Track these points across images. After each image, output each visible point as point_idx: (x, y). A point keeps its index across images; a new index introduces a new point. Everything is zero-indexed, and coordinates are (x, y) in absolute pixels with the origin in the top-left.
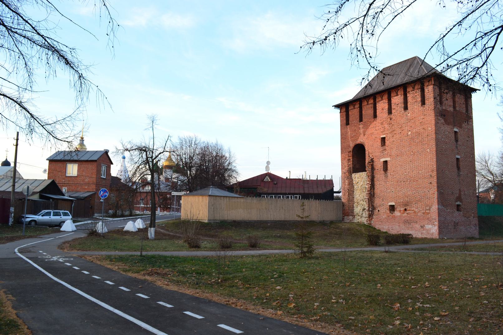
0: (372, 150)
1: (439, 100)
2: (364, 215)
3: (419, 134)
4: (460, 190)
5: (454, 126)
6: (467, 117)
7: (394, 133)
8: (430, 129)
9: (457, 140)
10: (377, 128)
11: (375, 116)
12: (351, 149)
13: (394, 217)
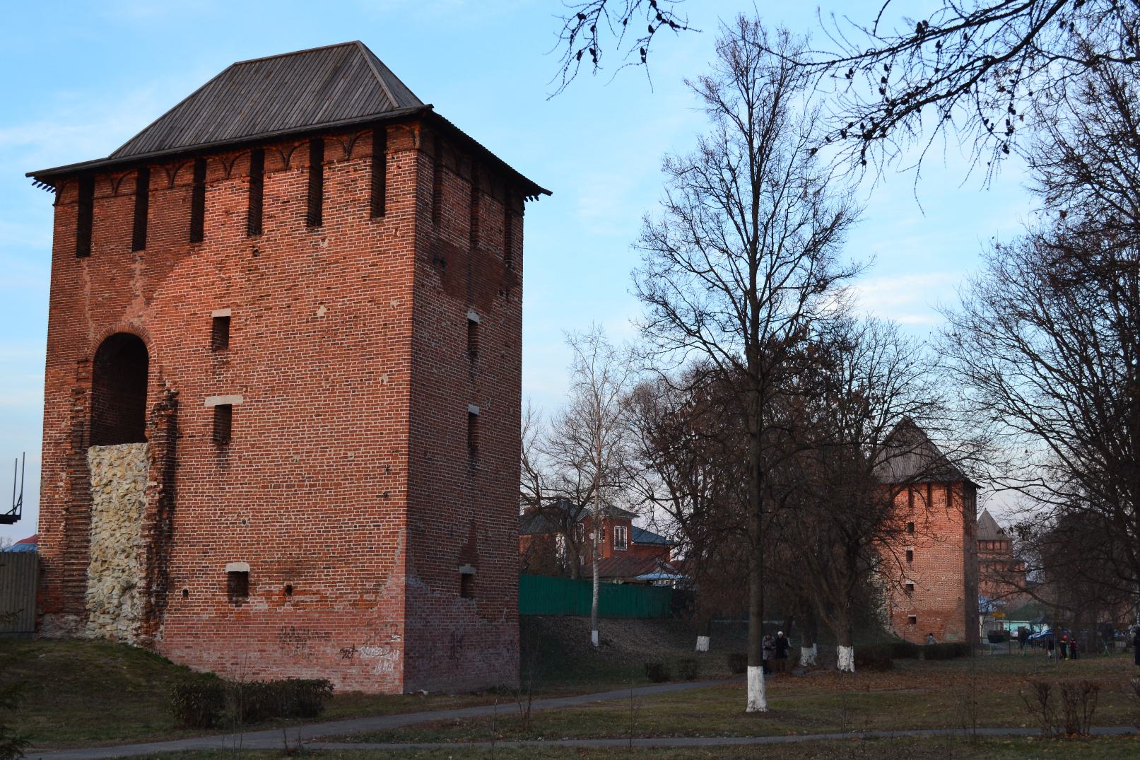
0: (174, 358)
1: (430, 208)
2: (127, 608)
3: (353, 317)
4: (472, 522)
5: (470, 302)
6: (508, 280)
7: (265, 304)
8: (394, 303)
9: (473, 354)
10: (201, 280)
11: (197, 234)
12: (89, 351)
13: (244, 618)
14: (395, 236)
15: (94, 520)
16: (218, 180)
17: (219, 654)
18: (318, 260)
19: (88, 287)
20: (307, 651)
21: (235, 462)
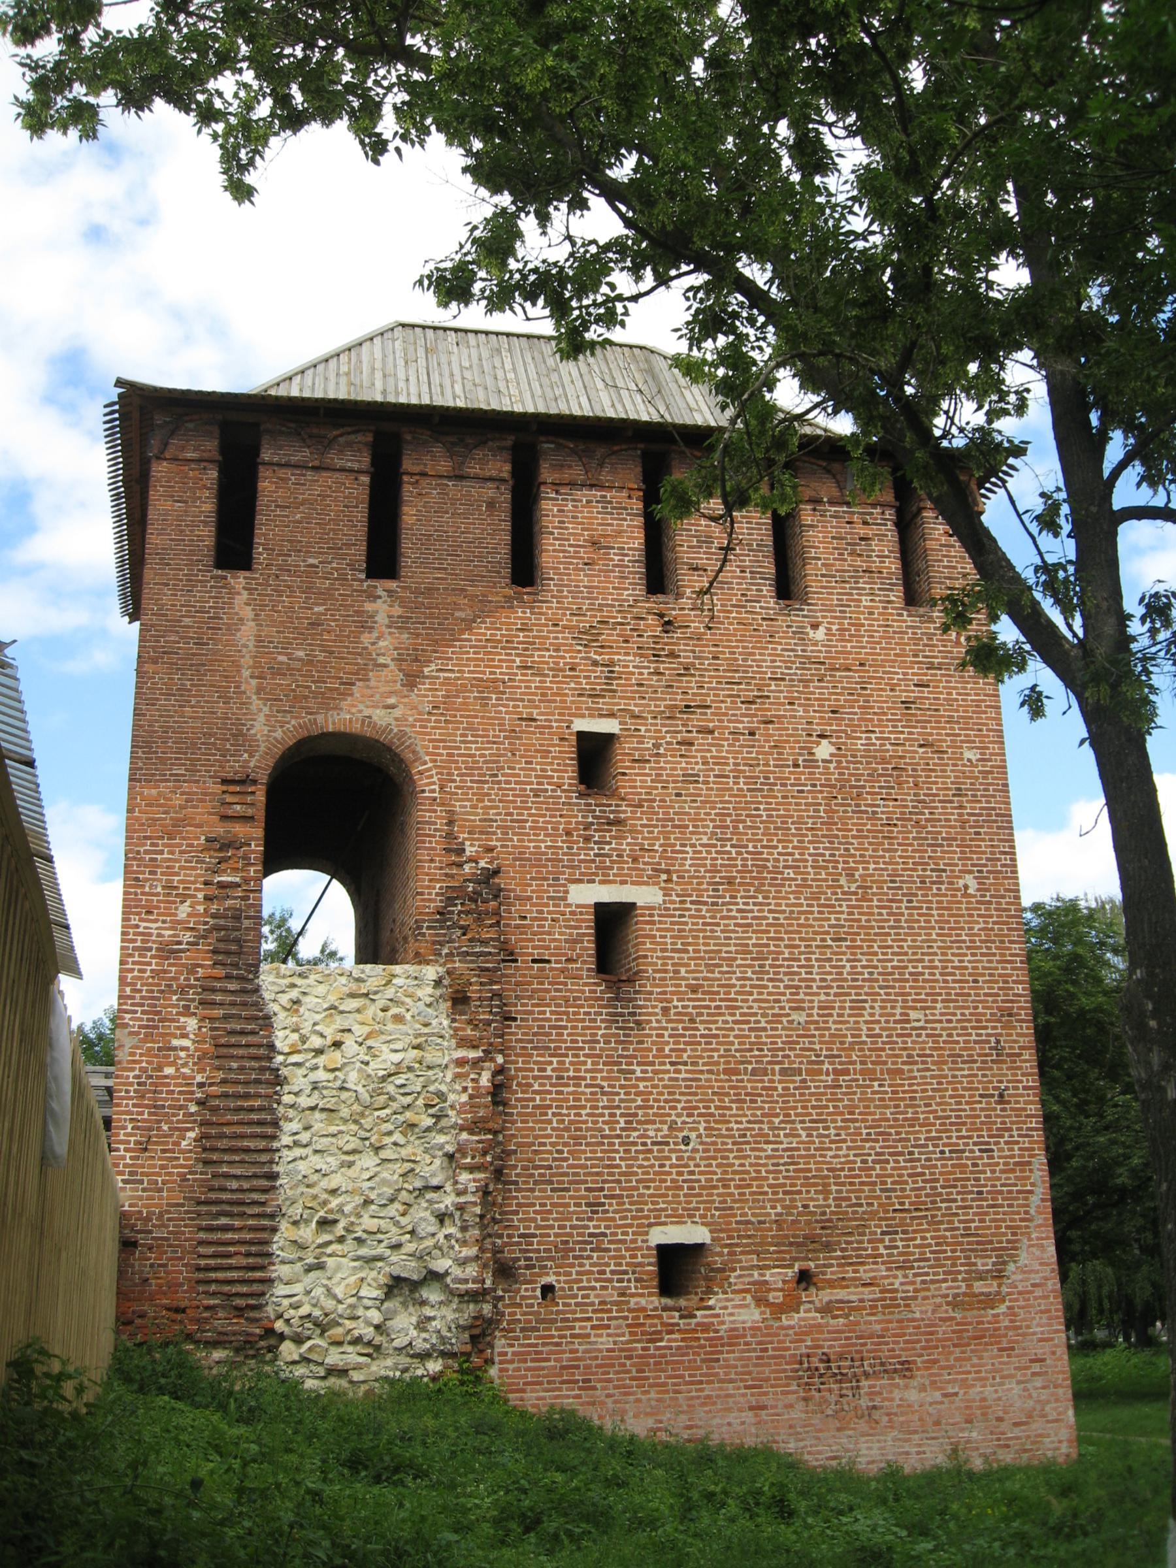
7: (696, 720)
11: (524, 569)
12: (259, 762)
15: (289, 1127)
16: (572, 484)
18: (809, 661)
19: (247, 634)
20: (864, 1402)
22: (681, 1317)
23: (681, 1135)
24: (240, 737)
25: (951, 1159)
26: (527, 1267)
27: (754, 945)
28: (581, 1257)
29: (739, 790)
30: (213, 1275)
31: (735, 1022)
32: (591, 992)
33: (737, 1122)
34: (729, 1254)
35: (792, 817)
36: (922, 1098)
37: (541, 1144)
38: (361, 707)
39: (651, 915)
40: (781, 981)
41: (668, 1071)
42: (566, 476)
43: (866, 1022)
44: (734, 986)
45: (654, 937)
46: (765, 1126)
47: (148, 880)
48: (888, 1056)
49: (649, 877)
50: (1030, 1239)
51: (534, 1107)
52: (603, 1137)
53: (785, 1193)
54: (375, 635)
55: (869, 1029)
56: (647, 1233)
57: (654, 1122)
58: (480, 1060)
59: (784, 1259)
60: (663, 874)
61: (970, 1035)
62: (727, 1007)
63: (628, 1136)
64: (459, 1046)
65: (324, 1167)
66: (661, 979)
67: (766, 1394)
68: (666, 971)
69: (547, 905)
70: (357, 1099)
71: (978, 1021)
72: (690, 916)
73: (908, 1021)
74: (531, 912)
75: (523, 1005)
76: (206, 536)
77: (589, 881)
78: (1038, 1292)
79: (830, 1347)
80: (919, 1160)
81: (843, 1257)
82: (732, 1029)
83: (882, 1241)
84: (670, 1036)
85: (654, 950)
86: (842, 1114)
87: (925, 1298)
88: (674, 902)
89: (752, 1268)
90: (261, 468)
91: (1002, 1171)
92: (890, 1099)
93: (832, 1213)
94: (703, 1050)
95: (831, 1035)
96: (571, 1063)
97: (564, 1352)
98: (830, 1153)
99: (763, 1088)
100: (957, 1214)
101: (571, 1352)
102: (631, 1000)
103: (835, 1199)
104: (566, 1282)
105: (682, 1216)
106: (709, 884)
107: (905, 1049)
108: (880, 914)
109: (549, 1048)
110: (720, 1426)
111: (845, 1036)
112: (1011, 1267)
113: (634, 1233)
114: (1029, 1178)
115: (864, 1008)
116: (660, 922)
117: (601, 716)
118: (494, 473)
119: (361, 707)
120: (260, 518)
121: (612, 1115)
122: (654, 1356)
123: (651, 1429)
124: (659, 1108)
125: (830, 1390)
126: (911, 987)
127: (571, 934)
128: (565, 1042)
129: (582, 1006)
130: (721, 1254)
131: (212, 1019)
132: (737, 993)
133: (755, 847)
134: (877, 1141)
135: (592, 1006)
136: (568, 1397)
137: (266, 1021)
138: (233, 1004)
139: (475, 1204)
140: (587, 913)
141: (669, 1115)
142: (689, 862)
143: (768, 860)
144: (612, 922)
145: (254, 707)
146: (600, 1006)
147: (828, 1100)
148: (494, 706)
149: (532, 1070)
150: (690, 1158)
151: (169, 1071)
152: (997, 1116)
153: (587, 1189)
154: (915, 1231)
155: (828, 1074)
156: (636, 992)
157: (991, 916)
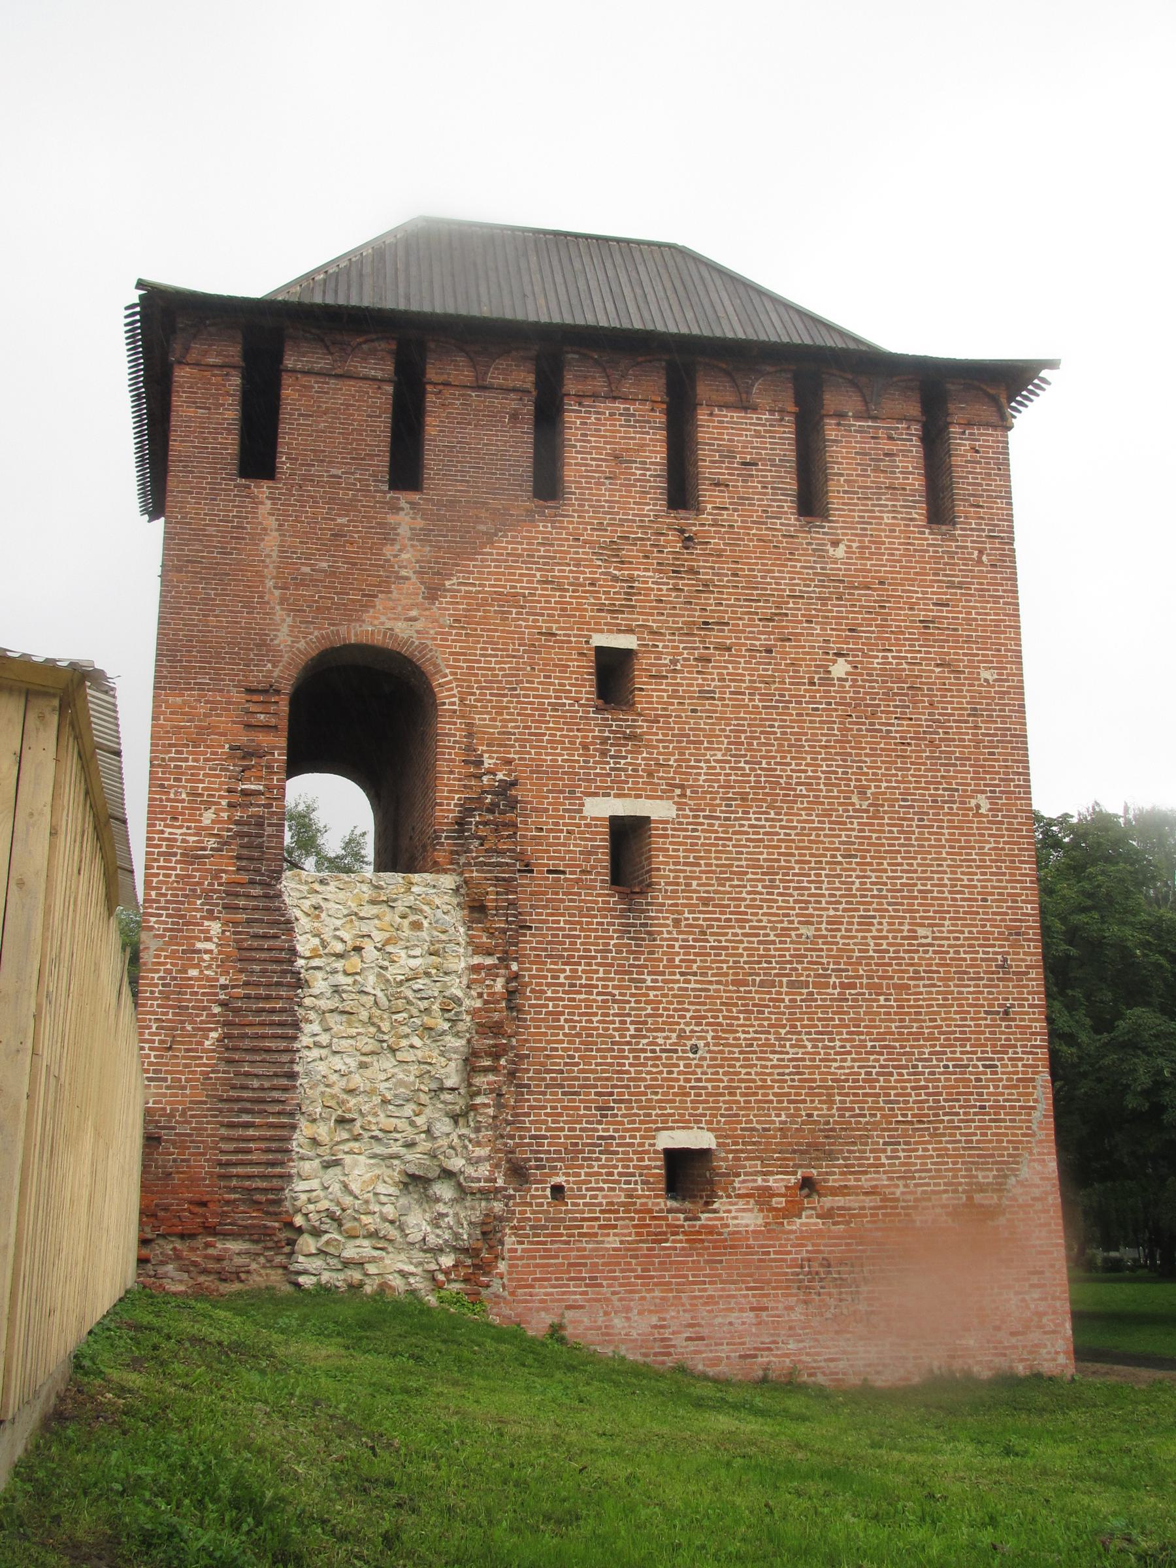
7: (714, 637)
11: (547, 484)
13: (721, 1243)
14: (979, 562)
15: (307, 1028)
16: (595, 396)
17: (654, 1320)
19: (271, 544)
20: (862, 1307)
21: (666, 931)
22: (686, 1219)
23: (689, 1043)
24: (264, 645)
25: (955, 1073)
26: (537, 1168)
27: (765, 860)
28: (590, 1159)
29: (754, 707)
30: (234, 1171)
31: (744, 935)
32: (604, 902)
33: (744, 1032)
34: (734, 1159)
35: (806, 734)
36: (927, 1013)
37: (553, 1049)
38: (383, 619)
39: (665, 829)
40: (791, 895)
41: (678, 981)
42: (588, 388)
43: (874, 938)
44: (744, 899)
45: (667, 850)
46: (772, 1037)
47: (171, 787)
48: (894, 971)
49: (663, 791)
50: (1031, 1154)
51: (547, 1013)
52: (613, 1043)
53: (789, 1102)
54: (397, 547)
55: (876, 944)
56: (654, 1137)
57: (663, 1030)
58: (495, 966)
59: (787, 1166)
60: (678, 789)
61: (977, 952)
62: (737, 920)
63: (637, 1043)
64: (475, 953)
65: (343, 1068)
66: (673, 891)
67: (768, 1295)
68: (678, 884)
69: (563, 817)
70: (376, 1002)
71: (985, 939)
72: (703, 831)
73: (916, 938)
74: (547, 823)
75: (537, 914)
76: (230, 444)
77: (604, 795)
78: (1039, 1206)
79: (830, 1252)
80: (923, 1073)
81: (846, 1166)
82: (742, 942)
83: (885, 1151)
84: (681, 947)
85: (667, 863)
86: (848, 1026)
87: (924, 1208)
88: (687, 817)
89: (756, 1173)
90: (285, 376)
91: (1005, 1087)
92: (896, 1013)
93: (836, 1122)
94: (713, 962)
95: (839, 950)
96: (583, 971)
97: (571, 1250)
98: (835, 1064)
99: (771, 1000)
100: (959, 1128)
101: (578, 1250)
102: (643, 911)
103: (839, 1109)
104: (575, 1183)
105: (689, 1121)
106: (722, 799)
107: (912, 965)
108: (891, 832)
109: (562, 957)
110: (721, 1325)
111: (853, 951)
112: (1013, 1180)
113: (642, 1137)
114: (1032, 1094)
115: (872, 924)
116: (673, 836)
117: (620, 631)
118: (518, 384)
119: (383, 619)
120: (283, 427)
121: (623, 1022)
122: (658, 1256)
123: (655, 1327)
124: (668, 1016)
125: (829, 1294)
126: (920, 905)
127: (586, 846)
128: (578, 950)
129: (595, 916)
130: (725, 1159)
131: (236, 924)
132: (747, 906)
133: (769, 763)
134: (882, 1054)
135: (605, 917)
136: (575, 1293)
137: (288, 926)
138: (255, 909)
139: (486, 1105)
140: (602, 826)
141: (678, 1024)
142: (703, 777)
143: (781, 777)
144: (627, 836)
145: (277, 618)
146: (613, 917)
147: (834, 1013)
148: (514, 620)
149: (546, 977)
150: (697, 1066)
151: (193, 973)
152: (1002, 1033)
153: (597, 1094)
154: (916, 1143)
155: (834, 987)
156: (648, 904)
157: (1002, 836)
